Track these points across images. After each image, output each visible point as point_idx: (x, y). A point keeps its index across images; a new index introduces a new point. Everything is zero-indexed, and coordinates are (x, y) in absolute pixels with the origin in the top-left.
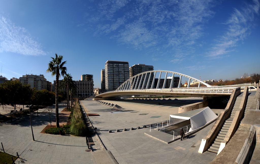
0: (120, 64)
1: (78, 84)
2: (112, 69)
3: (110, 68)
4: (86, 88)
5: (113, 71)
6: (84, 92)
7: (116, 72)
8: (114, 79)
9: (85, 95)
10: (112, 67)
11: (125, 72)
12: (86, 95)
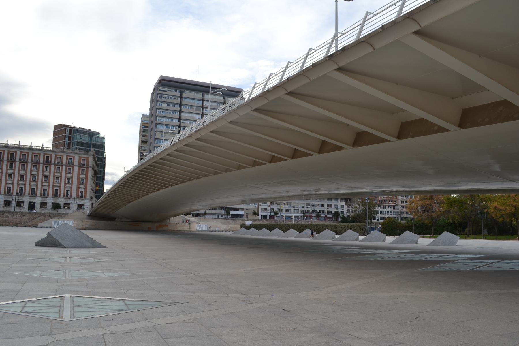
1: (23, 162)
2: (174, 112)
3: (168, 108)
4: (57, 178)
5: (180, 119)
6: (44, 195)
9: (50, 206)
10: (174, 105)
12: (56, 206)
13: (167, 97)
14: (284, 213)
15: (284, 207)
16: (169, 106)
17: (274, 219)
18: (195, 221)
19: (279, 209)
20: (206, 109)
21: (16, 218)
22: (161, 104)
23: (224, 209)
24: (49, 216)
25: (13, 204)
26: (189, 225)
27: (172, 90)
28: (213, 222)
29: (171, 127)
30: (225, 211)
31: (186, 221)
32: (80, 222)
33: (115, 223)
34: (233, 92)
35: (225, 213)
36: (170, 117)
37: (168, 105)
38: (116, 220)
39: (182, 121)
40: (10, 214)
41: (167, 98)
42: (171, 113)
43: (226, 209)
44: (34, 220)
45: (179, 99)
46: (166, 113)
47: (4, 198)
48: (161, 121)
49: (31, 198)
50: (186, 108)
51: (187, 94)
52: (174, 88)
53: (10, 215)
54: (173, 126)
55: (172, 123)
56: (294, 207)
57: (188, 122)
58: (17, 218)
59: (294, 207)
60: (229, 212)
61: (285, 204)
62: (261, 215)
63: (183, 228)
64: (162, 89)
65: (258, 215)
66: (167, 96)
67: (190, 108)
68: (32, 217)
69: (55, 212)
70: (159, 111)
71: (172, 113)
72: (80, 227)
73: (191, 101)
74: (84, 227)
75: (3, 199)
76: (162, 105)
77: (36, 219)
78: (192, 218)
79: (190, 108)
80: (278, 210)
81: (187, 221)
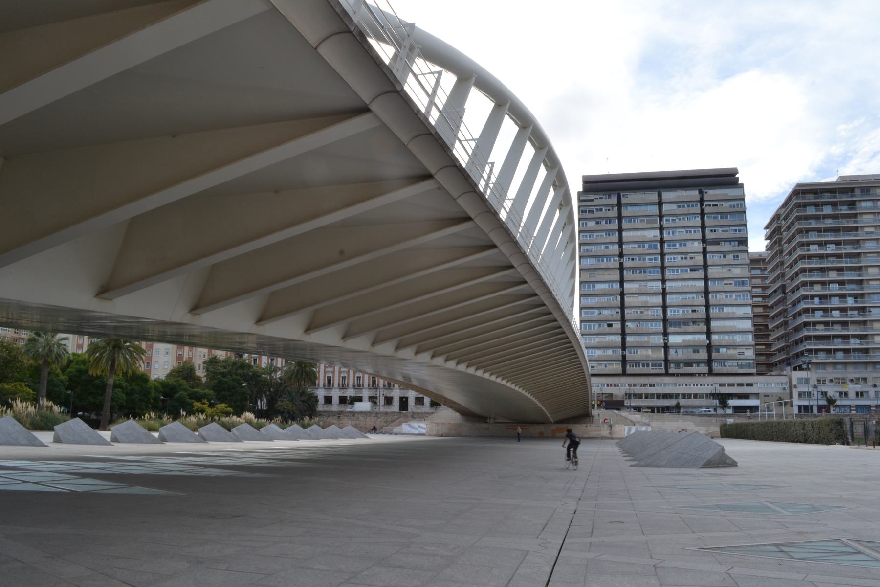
0: (667, 195)
2: (609, 232)
3: (599, 227)
7: (639, 251)
8: (627, 300)
10: (609, 220)
11: (710, 248)
13: (595, 209)
14: (852, 400)
15: (851, 386)
16: (599, 224)
17: (830, 412)
18: (643, 421)
19: (841, 393)
20: (667, 218)
21: (370, 420)
22: (586, 224)
23: (714, 395)
24: (412, 417)
25: (382, 401)
26: (609, 428)
27: (602, 196)
28: (678, 421)
29: (605, 259)
30: (717, 400)
31: (604, 421)
32: (434, 425)
33: (486, 425)
34: (716, 178)
35: (718, 404)
36: (603, 242)
37: (597, 223)
38: (488, 420)
39: (624, 246)
40: (362, 415)
41: (595, 211)
42: (604, 236)
43: (719, 397)
44: (393, 424)
45: (615, 209)
46: (595, 236)
47: (368, 393)
48: (588, 251)
49: (403, 391)
50: (629, 222)
51: (630, 198)
52: (605, 193)
53: (362, 416)
54: (608, 256)
55: (608, 252)
56: (875, 386)
57: (635, 246)
58: (370, 422)
59: (875, 386)
60: (726, 402)
61: (852, 381)
62: (800, 407)
63: (599, 433)
64: (585, 198)
65: (792, 406)
66: (594, 209)
67: (638, 221)
68: (389, 419)
69: (433, 410)
70: (582, 236)
71: (606, 234)
72: (434, 433)
73: (637, 208)
74: (440, 433)
75: (366, 395)
76: (588, 224)
77: (395, 422)
78: (636, 415)
79: (638, 221)
80: (838, 394)
81: (606, 421)
